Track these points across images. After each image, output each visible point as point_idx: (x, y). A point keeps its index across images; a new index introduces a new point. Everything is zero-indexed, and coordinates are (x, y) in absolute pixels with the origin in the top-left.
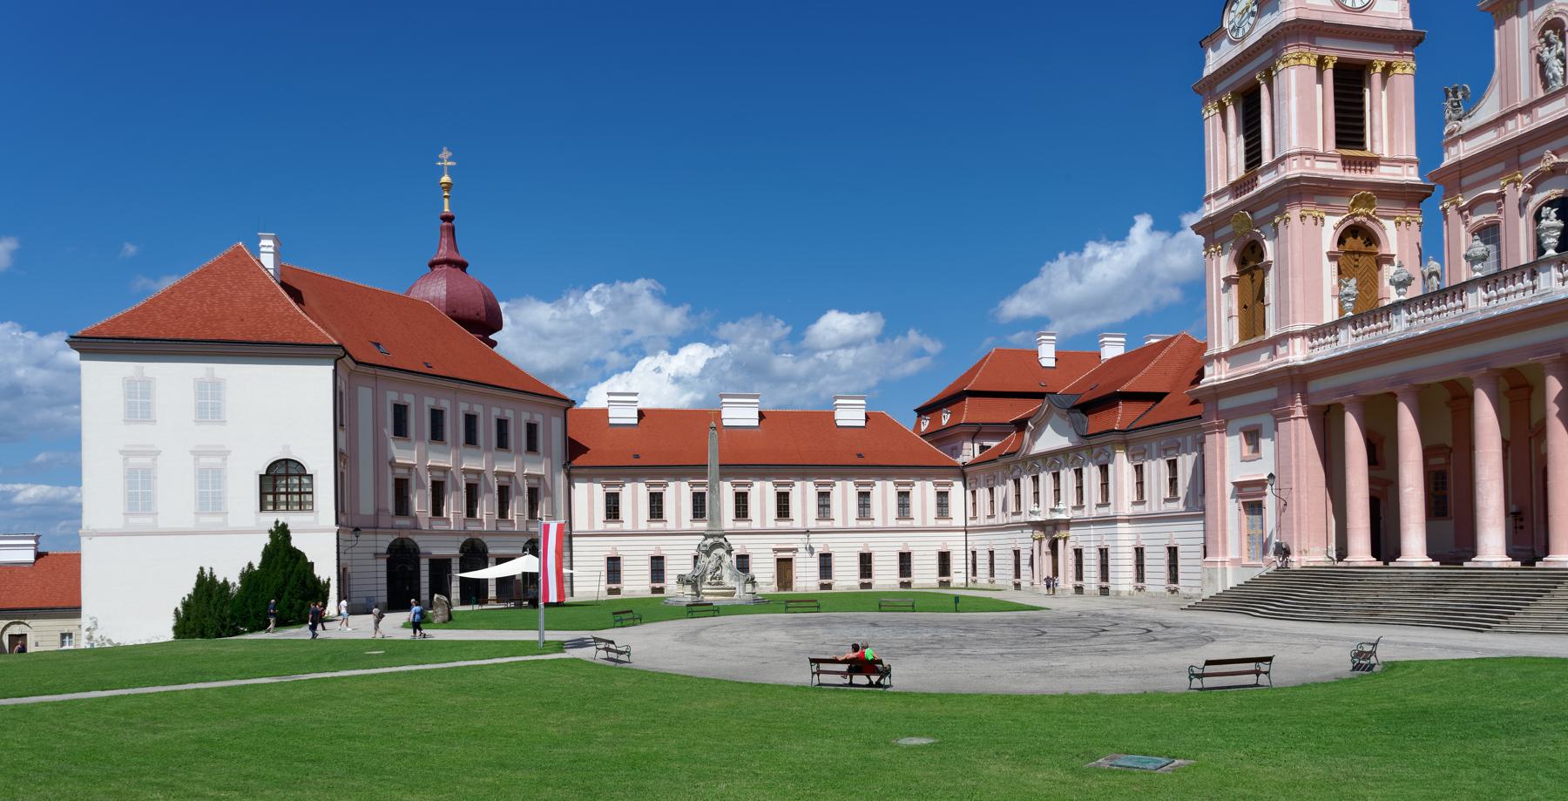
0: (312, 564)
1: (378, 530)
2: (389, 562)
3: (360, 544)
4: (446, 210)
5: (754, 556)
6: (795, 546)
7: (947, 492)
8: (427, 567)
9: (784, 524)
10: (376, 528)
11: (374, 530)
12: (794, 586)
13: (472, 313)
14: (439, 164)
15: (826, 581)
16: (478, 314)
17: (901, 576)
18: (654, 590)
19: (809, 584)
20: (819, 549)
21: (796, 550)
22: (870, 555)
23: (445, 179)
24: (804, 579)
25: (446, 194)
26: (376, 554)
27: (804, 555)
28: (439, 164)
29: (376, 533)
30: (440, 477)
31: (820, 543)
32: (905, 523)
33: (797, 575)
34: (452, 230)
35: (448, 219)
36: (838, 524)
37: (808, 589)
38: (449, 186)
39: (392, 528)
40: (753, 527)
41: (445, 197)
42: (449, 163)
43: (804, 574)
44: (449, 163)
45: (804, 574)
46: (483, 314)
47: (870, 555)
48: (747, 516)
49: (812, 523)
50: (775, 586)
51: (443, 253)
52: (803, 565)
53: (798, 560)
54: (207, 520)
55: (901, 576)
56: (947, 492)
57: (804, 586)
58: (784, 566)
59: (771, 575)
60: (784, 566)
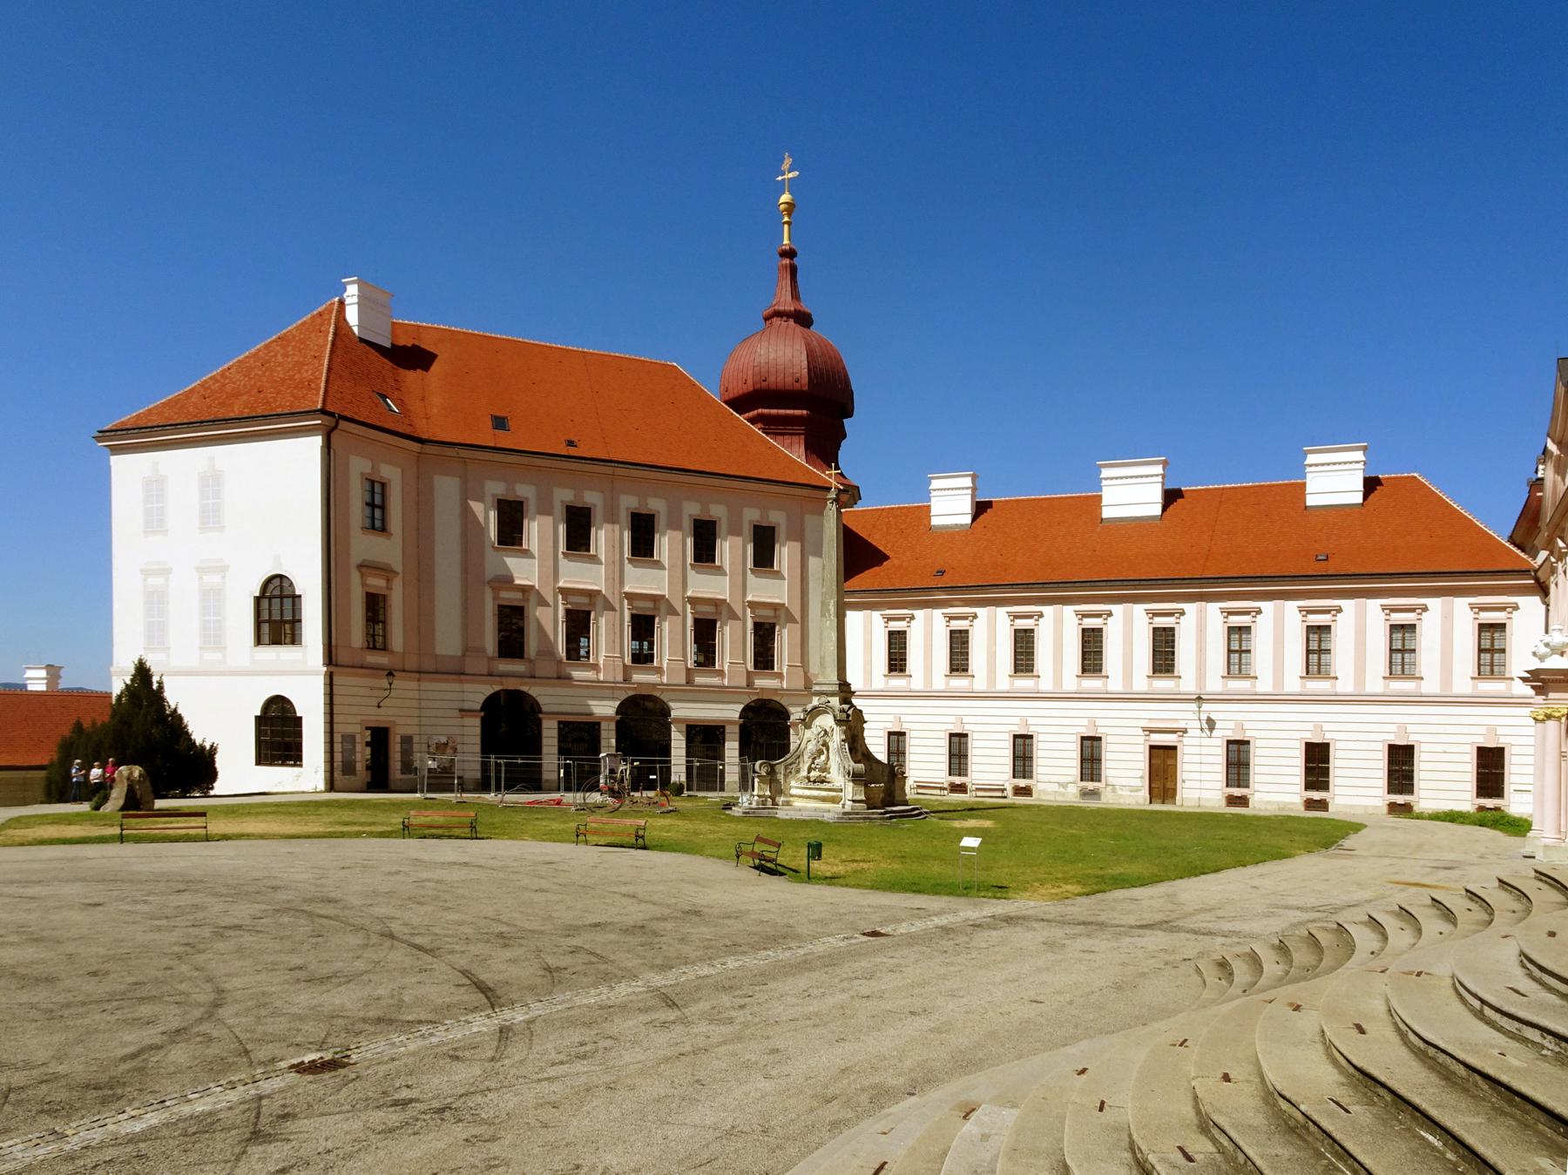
0: (301, 718)
1: (462, 677)
2: (483, 719)
3: (394, 693)
4: (786, 241)
5: (1110, 739)
6: (1182, 725)
7: (1414, 626)
8: (555, 733)
9: (1092, 684)
10: (459, 673)
11: (417, 675)
12: (1178, 797)
13: (789, 380)
14: (780, 178)
15: (1316, 795)
16: (797, 381)
17: (1390, 791)
18: (1019, 791)
19: (1206, 795)
20: (1226, 731)
21: (1185, 731)
22: (1500, 752)
23: (785, 198)
24: (1197, 785)
25: (786, 219)
26: (461, 710)
27: (1196, 741)
28: (780, 178)
29: (461, 681)
30: (647, 609)
31: (1231, 721)
32: (1318, 686)
33: (1185, 776)
34: (793, 271)
35: (790, 254)
36: (1264, 685)
37: (1202, 803)
38: (791, 207)
39: (490, 675)
40: (1110, 689)
41: (785, 223)
42: (791, 175)
43: (1197, 776)
44: (791, 175)
45: (1197, 776)
46: (805, 380)
47: (1500, 752)
48: (1101, 671)
49: (1215, 682)
50: (1145, 793)
51: (786, 303)
52: (1197, 758)
53: (1186, 750)
54: (213, 656)
55: (1390, 791)
56: (1414, 626)
57: (1197, 796)
58: (1162, 762)
59: (1140, 774)
60: (1162, 762)
